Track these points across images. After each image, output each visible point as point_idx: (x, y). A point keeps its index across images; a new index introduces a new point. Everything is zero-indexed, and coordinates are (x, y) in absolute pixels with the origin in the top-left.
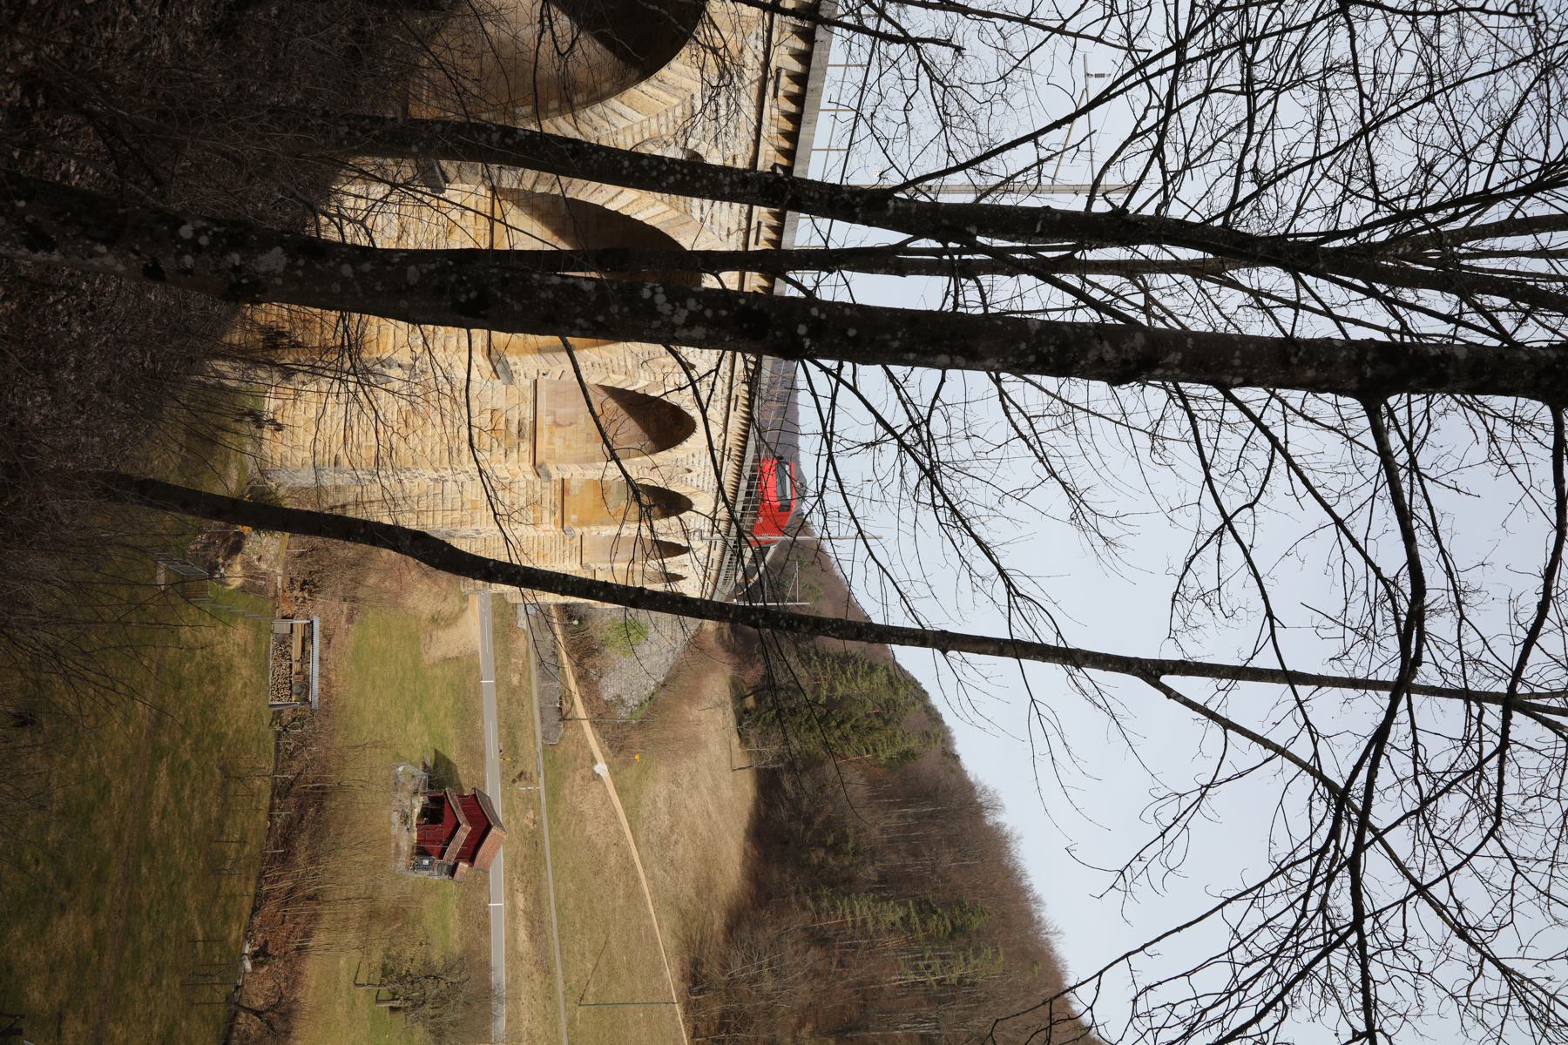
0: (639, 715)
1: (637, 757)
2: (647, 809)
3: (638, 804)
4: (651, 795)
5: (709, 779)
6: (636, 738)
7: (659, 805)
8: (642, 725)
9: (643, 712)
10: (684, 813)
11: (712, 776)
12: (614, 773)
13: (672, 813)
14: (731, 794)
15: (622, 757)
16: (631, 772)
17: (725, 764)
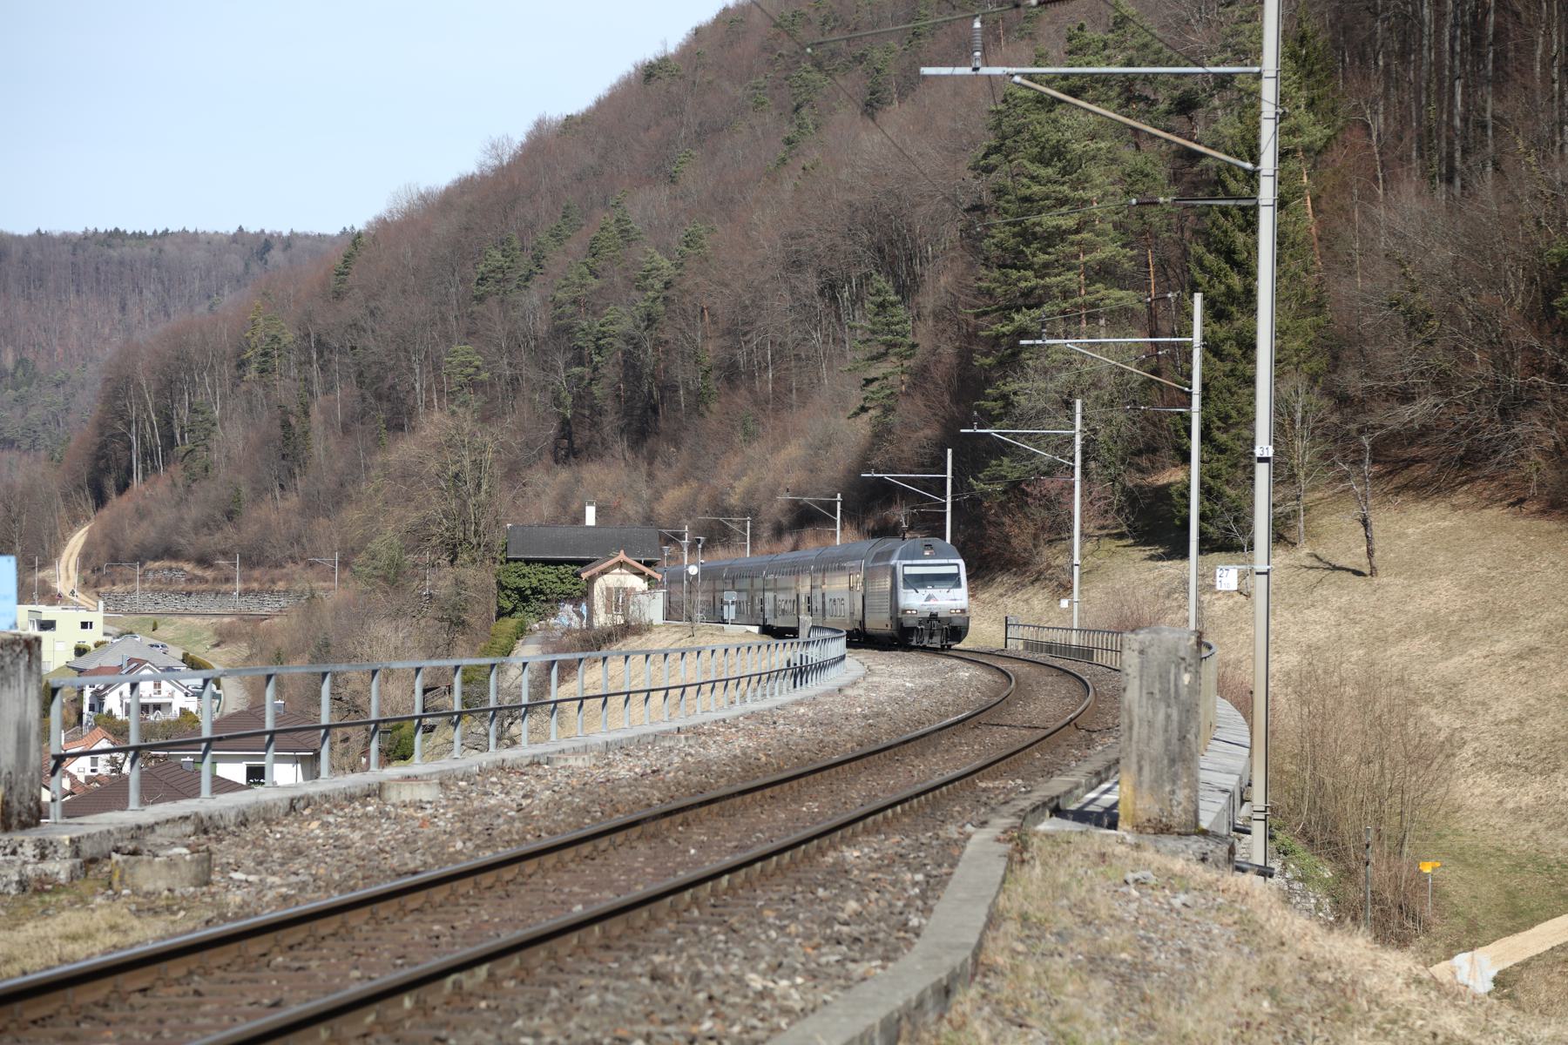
0: (1309, 859)
1: (1427, 868)
2: (1546, 838)
3: (1538, 862)
4: (1501, 822)
5: (1415, 646)
6: (1378, 872)
7: (1528, 800)
8: (1333, 850)
9: (1299, 846)
10: (1540, 727)
11: (1403, 635)
12: (1472, 937)
13: (1547, 761)
14: (1445, 582)
15: (1428, 911)
16: (1459, 885)
17: (1356, 593)
